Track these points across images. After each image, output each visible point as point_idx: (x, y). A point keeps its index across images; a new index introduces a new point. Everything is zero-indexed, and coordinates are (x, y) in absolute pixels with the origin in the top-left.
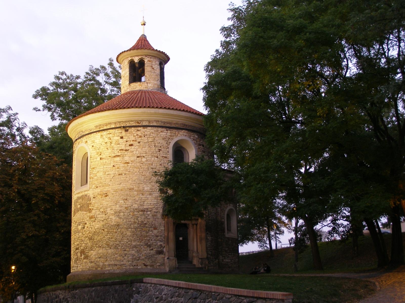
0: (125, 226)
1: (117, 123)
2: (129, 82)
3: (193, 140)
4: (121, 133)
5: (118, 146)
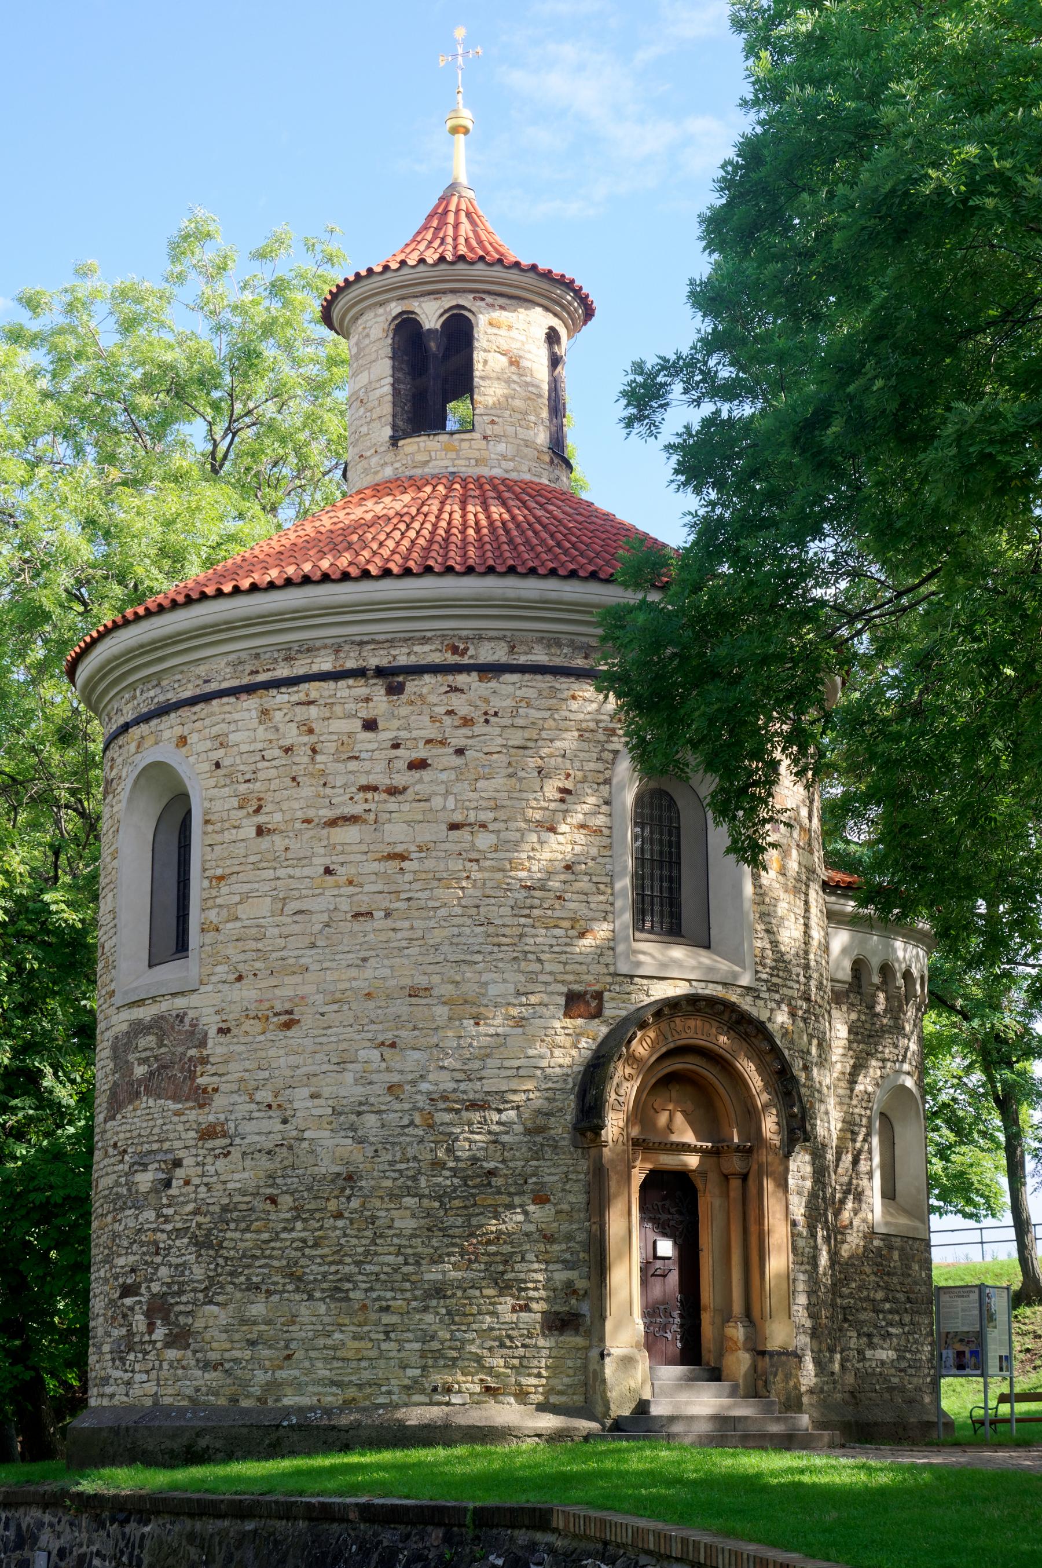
0: (388, 1183)
1: (346, 648)
2: (394, 427)
4: (368, 700)
5: (353, 765)
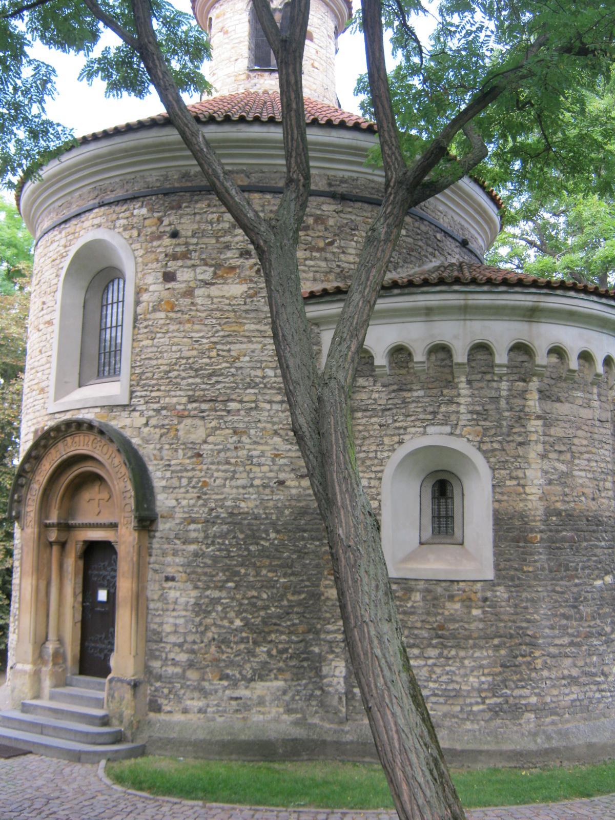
3: (125, 230)
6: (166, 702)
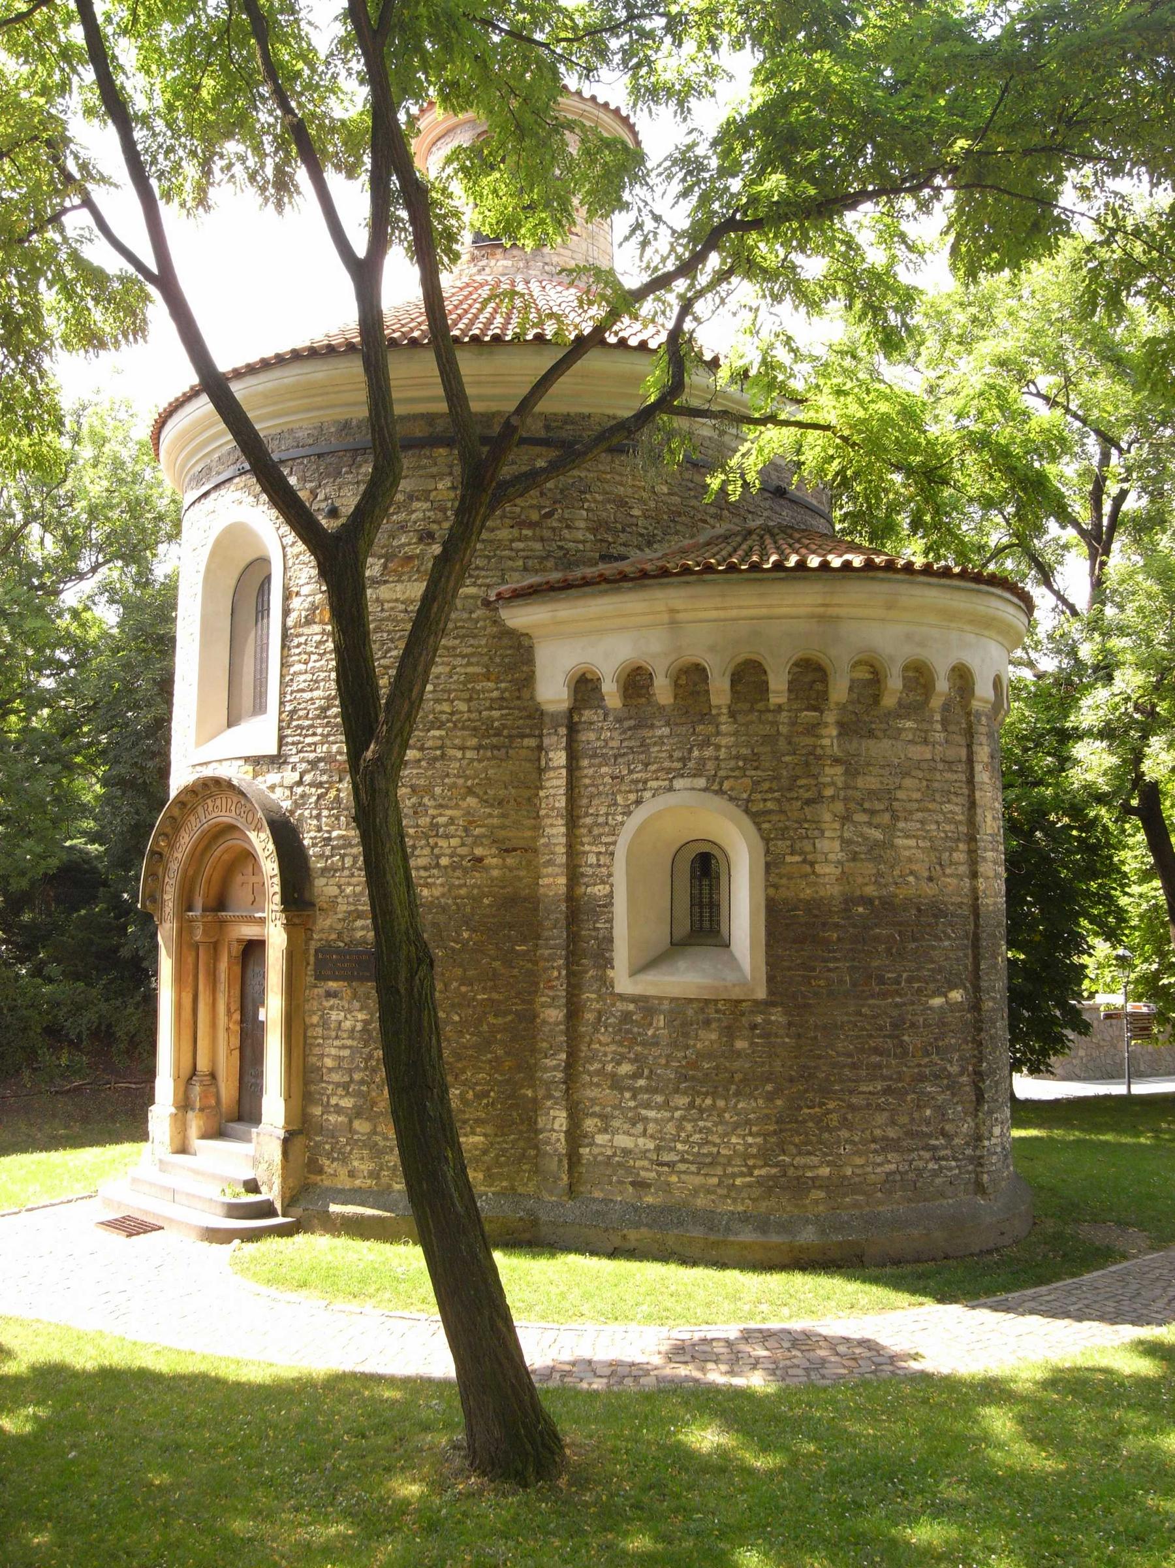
6: (327, 1162)
